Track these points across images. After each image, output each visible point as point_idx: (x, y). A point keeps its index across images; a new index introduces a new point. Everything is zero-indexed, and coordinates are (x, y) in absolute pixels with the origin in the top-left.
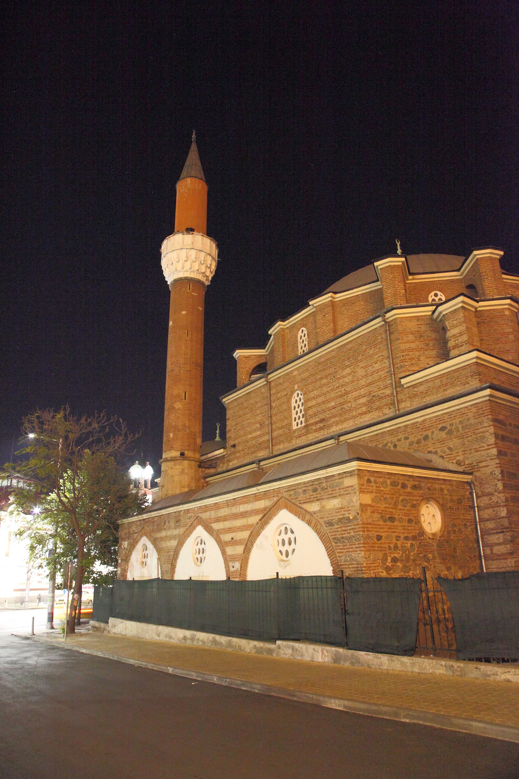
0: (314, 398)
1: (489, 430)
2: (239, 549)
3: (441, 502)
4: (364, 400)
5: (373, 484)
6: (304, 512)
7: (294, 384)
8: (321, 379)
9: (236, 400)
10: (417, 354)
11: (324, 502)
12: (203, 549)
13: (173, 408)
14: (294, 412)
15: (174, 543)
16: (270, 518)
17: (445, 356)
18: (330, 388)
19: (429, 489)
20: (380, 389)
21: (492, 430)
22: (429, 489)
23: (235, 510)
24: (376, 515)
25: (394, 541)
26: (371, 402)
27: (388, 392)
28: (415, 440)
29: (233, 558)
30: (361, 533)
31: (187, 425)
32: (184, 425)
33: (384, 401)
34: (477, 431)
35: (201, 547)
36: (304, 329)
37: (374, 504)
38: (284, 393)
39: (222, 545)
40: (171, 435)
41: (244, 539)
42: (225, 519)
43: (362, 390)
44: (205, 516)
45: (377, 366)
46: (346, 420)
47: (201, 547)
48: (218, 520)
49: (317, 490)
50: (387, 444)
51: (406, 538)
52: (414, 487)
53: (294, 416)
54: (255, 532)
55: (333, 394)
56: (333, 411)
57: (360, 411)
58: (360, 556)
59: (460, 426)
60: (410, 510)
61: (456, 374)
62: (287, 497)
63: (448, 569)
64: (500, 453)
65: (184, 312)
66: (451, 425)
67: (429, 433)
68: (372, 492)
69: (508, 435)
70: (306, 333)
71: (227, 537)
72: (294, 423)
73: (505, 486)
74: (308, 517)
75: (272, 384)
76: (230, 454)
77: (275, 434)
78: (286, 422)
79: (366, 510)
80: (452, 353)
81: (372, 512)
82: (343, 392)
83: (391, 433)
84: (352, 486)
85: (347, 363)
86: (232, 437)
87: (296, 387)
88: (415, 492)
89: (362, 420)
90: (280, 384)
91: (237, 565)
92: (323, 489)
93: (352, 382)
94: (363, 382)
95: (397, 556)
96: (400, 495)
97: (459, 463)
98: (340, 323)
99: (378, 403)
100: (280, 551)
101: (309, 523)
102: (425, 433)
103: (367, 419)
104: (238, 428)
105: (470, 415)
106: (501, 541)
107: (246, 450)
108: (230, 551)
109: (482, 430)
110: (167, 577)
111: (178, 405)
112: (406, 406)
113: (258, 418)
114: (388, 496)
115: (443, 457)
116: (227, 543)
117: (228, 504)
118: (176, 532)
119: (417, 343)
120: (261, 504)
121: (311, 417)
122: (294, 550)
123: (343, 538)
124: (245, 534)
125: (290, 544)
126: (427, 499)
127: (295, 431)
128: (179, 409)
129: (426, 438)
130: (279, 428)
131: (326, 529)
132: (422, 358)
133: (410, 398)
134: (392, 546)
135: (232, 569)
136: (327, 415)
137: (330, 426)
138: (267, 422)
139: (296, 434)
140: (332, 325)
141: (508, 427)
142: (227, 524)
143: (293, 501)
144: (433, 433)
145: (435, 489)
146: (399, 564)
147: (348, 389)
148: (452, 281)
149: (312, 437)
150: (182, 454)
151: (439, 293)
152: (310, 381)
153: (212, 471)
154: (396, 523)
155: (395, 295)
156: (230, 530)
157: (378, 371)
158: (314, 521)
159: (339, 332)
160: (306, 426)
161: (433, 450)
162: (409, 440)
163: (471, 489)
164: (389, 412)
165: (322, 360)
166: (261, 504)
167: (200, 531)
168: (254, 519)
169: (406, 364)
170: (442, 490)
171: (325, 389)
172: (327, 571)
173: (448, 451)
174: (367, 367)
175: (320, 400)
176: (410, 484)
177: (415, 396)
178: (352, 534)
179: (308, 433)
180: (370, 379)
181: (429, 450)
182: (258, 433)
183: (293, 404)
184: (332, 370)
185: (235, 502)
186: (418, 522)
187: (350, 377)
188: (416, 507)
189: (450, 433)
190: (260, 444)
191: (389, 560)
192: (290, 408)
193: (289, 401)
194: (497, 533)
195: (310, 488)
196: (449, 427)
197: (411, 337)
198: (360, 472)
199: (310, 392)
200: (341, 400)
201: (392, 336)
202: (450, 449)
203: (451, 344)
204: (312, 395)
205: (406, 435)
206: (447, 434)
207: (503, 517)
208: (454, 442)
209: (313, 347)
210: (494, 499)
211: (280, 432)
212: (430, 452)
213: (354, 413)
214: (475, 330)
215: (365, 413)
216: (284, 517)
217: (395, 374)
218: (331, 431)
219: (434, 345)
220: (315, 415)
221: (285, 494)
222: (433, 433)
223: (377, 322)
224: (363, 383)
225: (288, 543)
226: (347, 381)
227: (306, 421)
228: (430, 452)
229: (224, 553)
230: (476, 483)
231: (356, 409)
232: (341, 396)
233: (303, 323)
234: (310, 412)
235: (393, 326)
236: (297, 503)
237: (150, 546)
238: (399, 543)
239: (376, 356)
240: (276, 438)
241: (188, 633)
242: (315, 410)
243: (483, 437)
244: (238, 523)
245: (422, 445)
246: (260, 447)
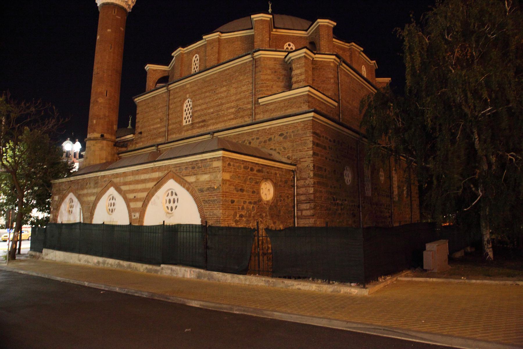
0: (200, 105)
1: (309, 139)
2: (139, 204)
3: (275, 181)
4: (233, 110)
5: (232, 167)
6: (185, 182)
7: (187, 94)
8: (206, 92)
9: (145, 100)
10: (272, 83)
11: (199, 177)
12: (114, 204)
13: (97, 102)
14: (185, 113)
15: (93, 198)
16: (162, 185)
17: (289, 87)
18: (211, 100)
19: (268, 172)
20: (244, 104)
21: (311, 139)
22: (268, 172)
23: (137, 178)
24: (232, 187)
25: (242, 204)
26: (237, 112)
27: (249, 106)
28: (263, 140)
29: (135, 210)
30: (221, 198)
31: (107, 115)
32: (105, 115)
33: (246, 113)
34: (302, 139)
35: (112, 202)
36: (197, 55)
37: (231, 180)
38: (179, 99)
39: (128, 201)
40: (95, 122)
41: (143, 198)
42: (130, 183)
43: (233, 103)
44: (116, 180)
45: (244, 88)
46: (220, 122)
47: (112, 202)
48: (125, 184)
49: (195, 168)
50: (244, 141)
51: (250, 203)
52: (259, 171)
53: (184, 116)
54: (151, 193)
55: (212, 104)
56: (211, 115)
57: (229, 117)
58: (219, 212)
59: (292, 134)
60: (254, 185)
61: (294, 100)
62: (174, 171)
63: (274, 223)
64: (314, 154)
65: (109, 30)
66: (287, 133)
67: (272, 137)
68: (231, 172)
69: (321, 143)
70: (198, 58)
71: (131, 196)
72: (184, 121)
73: (315, 175)
74: (187, 185)
75: (171, 92)
76: (138, 139)
77: (170, 127)
78: (179, 119)
79: (226, 183)
80: (294, 86)
81: (230, 185)
82: (220, 102)
83: (249, 134)
84: (218, 167)
85: (224, 83)
86: (140, 126)
87: (188, 96)
88: (259, 174)
89: (230, 123)
90: (177, 92)
91: (137, 215)
92: (199, 167)
93: (226, 97)
94: (233, 98)
95: (243, 213)
96: (249, 175)
97: (288, 158)
98: (222, 55)
99: (241, 113)
100: (167, 207)
101: (188, 189)
102: (270, 137)
103: (234, 123)
104: (145, 120)
105: (299, 128)
106: (308, 208)
107: (149, 137)
108: (132, 205)
109: (305, 138)
110: (87, 222)
111: (101, 100)
112: (260, 117)
113: (159, 115)
114: (241, 175)
115: (279, 153)
116: (131, 200)
117: (133, 173)
118: (95, 191)
119: (273, 76)
120: (156, 175)
121: (196, 118)
122: (176, 207)
123: (209, 200)
124: (144, 195)
125: (174, 202)
126: (266, 179)
127: (184, 126)
128: (101, 103)
129: (270, 139)
130: (174, 124)
131: (198, 194)
132: (274, 87)
133: (263, 112)
134: (241, 207)
135: (133, 218)
136: (207, 118)
137: (208, 126)
138: (165, 119)
139: (185, 128)
140: (217, 55)
141: (322, 138)
142: (132, 187)
143: (178, 174)
144: (275, 137)
145: (272, 173)
146: (244, 218)
147: (224, 101)
148: (301, 37)
149: (196, 132)
150: (102, 136)
151: (291, 44)
152: (197, 92)
153: (124, 149)
154: (244, 193)
155: (262, 41)
156: (133, 191)
157: (244, 92)
158: (191, 188)
159: (222, 61)
160: (192, 124)
161: (274, 148)
162: (258, 141)
163: (294, 175)
164: (248, 120)
165: (208, 79)
166: (156, 175)
167: (112, 191)
168: (151, 185)
169: (263, 89)
170: (276, 174)
171: (207, 100)
173: (283, 150)
175: (204, 106)
176: (256, 168)
177: (267, 111)
178: (215, 198)
179: (193, 128)
180: (239, 97)
181: (271, 147)
182: (159, 125)
183: (185, 108)
184: (214, 87)
185: (138, 172)
186: (259, 193)
187: (225, 94)
188: (258, 183)
189: (285, 138)
190: (159, 133)
191: (238, 215)
192: (182, 109)
193: (182, 105)
194: (306, 203)
195: (190, 166)
196: (285, 134)
197: (269, 72)
198: (224, 158)
199: (197, 100)
200: (218, 109)
201: (257, 69)
202: (284, 148)
203: (294, 80)
204: (198, 103)
205: (258, 137)
206: (283, 138)
207: (311, 194)
208: (288, 144)
209: (202, 69)
210: (307, 182)
211: (174, 126)
212: (271, 149)
213: (225, 118)
214: (310, 73)
215: (233, 119)
216: (171, 184)
217: (255, 95)
218: (209, 128)
219: (283, 79)
220: (199, 117)
221: (172, 169)
222: (275, 137)
223: (248, 58)
224: (234, 99)
226: (223, 96)
227: (193, 120)
228: (271, 149)
229: (128, 206)
230: (298, 172)
231: (227, 115)
232: (218, 106)
233: (197, 51)
234: (196, 115)
235: (258, 62)
236: (181, 176)
237: (75, 200)
238: (245, 206)
239: (244, 81)
240: (171, 130)
241: (101, 259)
242: (199, 113)
243: (305, 143)
244: (140, 186)
245: (267, 144)
246: (159, 135)
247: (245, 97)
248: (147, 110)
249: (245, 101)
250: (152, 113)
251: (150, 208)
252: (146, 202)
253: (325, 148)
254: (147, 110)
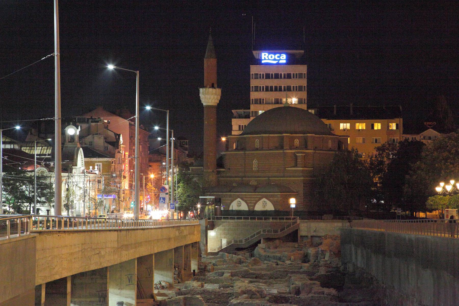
15: (230, 201)
17: (296, 166)
29: (251, 206)
42: (248, 198)
44: (241, 196)
48: (246, 198)
49: (272, 196)
54: (257, 202)
80: (298, 165)
91: (252, 207)
108: (249, 204)
117: (249, 195)
118: (230, 199)
120: (259, 196)
124: (255, 202)
142: (249, 199)
149: (259, 174)
166: (259, 196)
167: (239, 199)
172: (273, 209)
185: (252, 195)
203: (298, 163)
216: (264, 199)
225: (265, 205)
233: (258, 138)
251: (257, 206)
252: (255, 204)
253: (307, 187)
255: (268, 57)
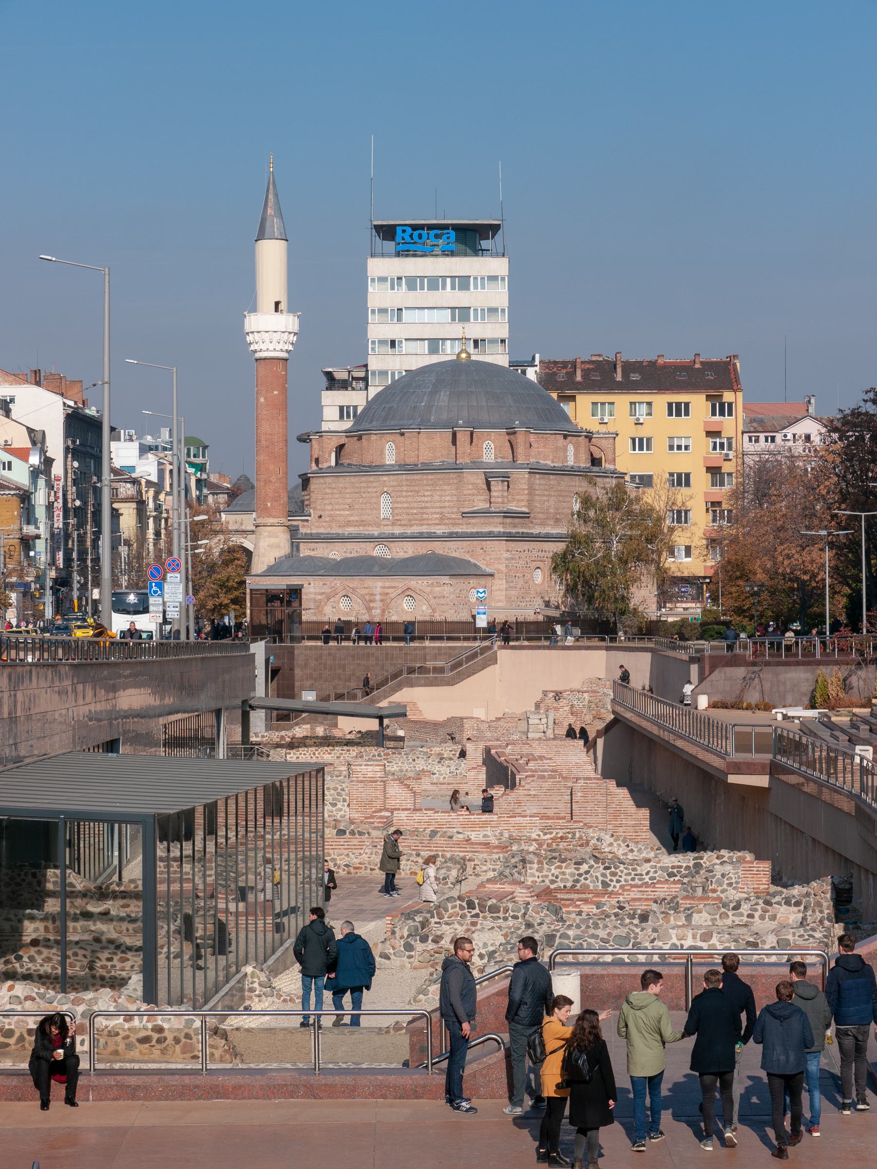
4: (438, 516)
8: (407, 491)
20: (448, 513)
38: (375, 490)
40: (269, 504)
55: (415, 505)
65: (276, 392)
86: (319, 507)
94: (438, 504)
157: (448, 501)
171: (409, 499)
174: (441, 496)
175: (405, 505)
179: (393, 524)
180: (443, 504)
182: (347, 512)
184: (417, 488)
187: (429, 499)
197: (471, 487)
200: (422, 511)
204: (399, 499)
232: (422, 508)
247: (449, 507)
248: (328, 491)
249: (450, 510)
250: (337, 496)
254: (328, 491)
255: (411, 236)
